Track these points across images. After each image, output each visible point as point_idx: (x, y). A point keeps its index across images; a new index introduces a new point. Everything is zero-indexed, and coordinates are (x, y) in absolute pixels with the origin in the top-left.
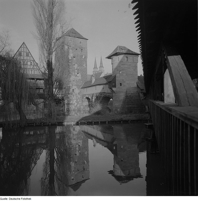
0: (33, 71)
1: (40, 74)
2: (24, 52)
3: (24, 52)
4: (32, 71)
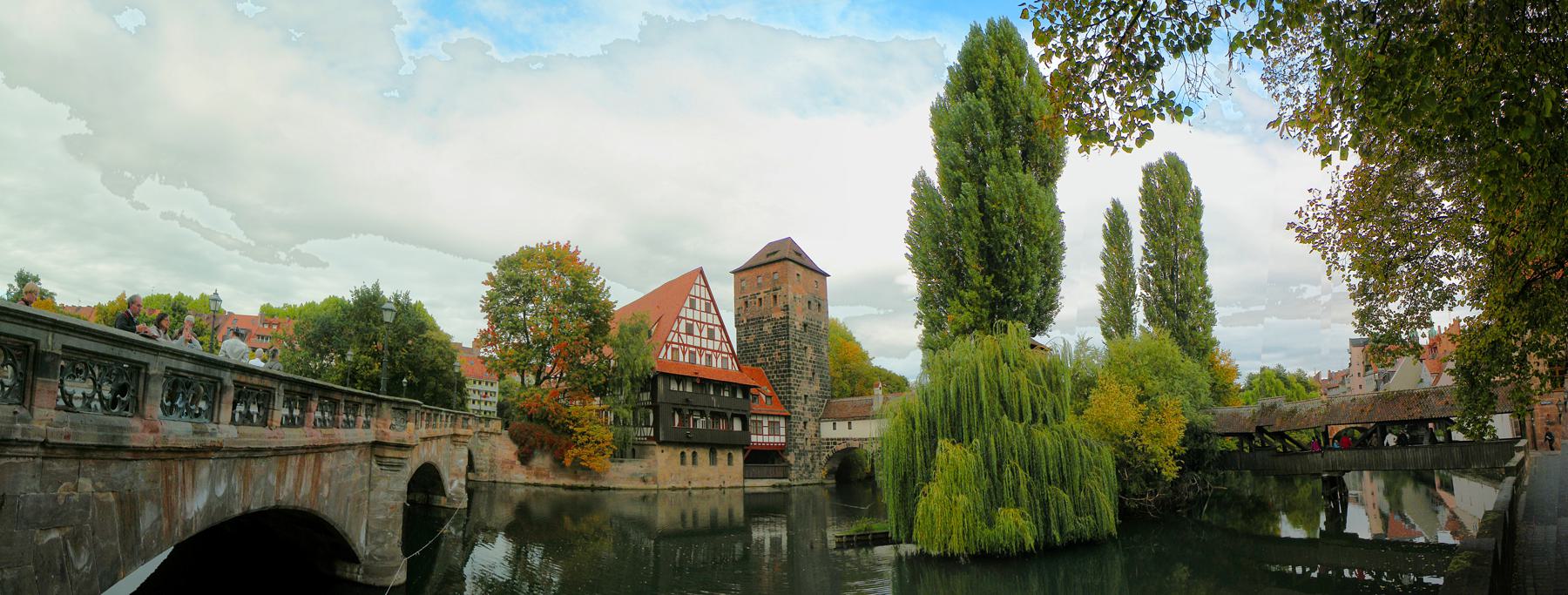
0: (720, 359)
2: (700, 298)
3: (700, 298)
4: (717, 358)
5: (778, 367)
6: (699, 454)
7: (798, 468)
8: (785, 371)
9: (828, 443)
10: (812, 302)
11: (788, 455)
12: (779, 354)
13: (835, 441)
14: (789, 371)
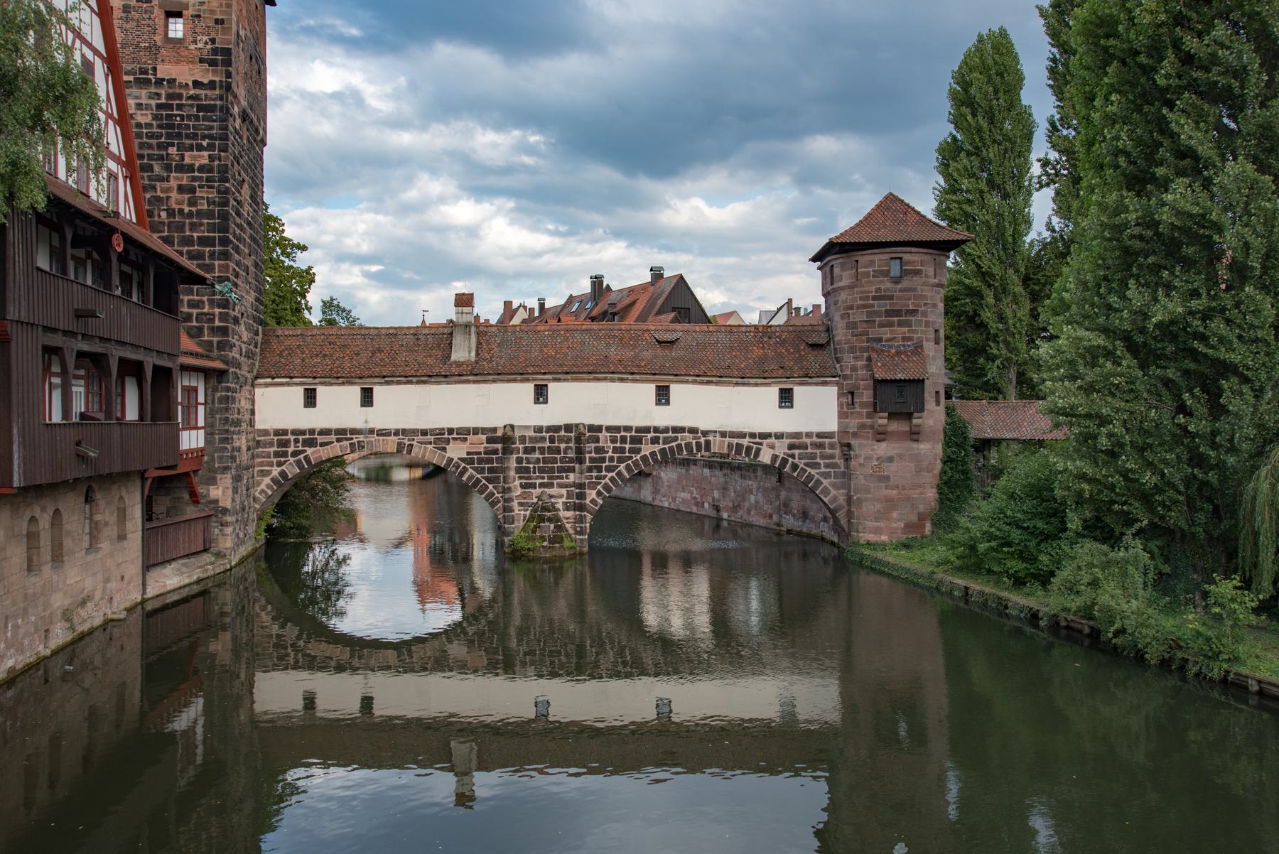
1: (128, 217)
5: (181, 228)
6: (65, 516)
7: (234, 519)
8: (203, 241)
9: (285, 444)
10: (254, 60)
11: (212, 481)
12: (181, 189)
13: (310, 438)
14: (225, 242)
